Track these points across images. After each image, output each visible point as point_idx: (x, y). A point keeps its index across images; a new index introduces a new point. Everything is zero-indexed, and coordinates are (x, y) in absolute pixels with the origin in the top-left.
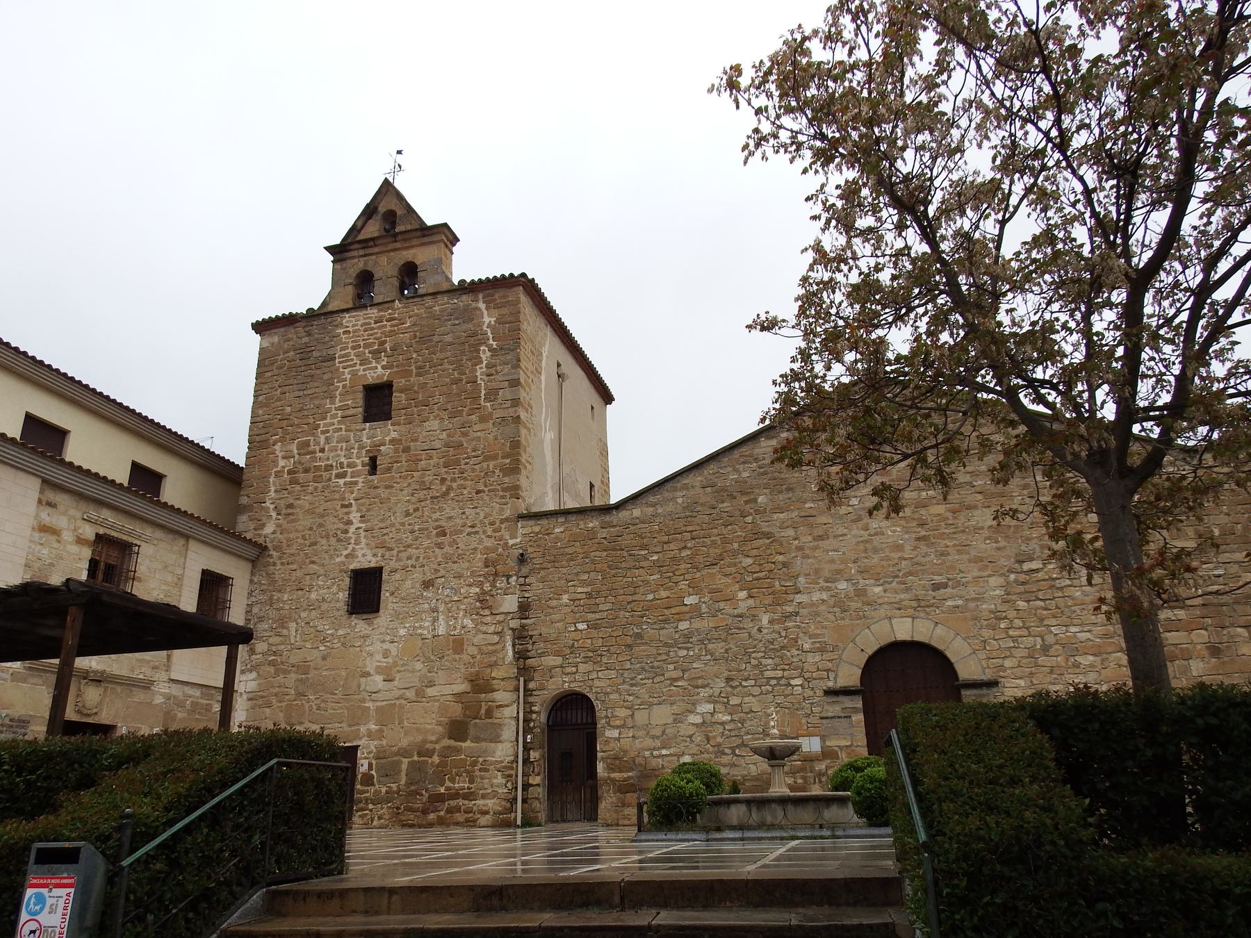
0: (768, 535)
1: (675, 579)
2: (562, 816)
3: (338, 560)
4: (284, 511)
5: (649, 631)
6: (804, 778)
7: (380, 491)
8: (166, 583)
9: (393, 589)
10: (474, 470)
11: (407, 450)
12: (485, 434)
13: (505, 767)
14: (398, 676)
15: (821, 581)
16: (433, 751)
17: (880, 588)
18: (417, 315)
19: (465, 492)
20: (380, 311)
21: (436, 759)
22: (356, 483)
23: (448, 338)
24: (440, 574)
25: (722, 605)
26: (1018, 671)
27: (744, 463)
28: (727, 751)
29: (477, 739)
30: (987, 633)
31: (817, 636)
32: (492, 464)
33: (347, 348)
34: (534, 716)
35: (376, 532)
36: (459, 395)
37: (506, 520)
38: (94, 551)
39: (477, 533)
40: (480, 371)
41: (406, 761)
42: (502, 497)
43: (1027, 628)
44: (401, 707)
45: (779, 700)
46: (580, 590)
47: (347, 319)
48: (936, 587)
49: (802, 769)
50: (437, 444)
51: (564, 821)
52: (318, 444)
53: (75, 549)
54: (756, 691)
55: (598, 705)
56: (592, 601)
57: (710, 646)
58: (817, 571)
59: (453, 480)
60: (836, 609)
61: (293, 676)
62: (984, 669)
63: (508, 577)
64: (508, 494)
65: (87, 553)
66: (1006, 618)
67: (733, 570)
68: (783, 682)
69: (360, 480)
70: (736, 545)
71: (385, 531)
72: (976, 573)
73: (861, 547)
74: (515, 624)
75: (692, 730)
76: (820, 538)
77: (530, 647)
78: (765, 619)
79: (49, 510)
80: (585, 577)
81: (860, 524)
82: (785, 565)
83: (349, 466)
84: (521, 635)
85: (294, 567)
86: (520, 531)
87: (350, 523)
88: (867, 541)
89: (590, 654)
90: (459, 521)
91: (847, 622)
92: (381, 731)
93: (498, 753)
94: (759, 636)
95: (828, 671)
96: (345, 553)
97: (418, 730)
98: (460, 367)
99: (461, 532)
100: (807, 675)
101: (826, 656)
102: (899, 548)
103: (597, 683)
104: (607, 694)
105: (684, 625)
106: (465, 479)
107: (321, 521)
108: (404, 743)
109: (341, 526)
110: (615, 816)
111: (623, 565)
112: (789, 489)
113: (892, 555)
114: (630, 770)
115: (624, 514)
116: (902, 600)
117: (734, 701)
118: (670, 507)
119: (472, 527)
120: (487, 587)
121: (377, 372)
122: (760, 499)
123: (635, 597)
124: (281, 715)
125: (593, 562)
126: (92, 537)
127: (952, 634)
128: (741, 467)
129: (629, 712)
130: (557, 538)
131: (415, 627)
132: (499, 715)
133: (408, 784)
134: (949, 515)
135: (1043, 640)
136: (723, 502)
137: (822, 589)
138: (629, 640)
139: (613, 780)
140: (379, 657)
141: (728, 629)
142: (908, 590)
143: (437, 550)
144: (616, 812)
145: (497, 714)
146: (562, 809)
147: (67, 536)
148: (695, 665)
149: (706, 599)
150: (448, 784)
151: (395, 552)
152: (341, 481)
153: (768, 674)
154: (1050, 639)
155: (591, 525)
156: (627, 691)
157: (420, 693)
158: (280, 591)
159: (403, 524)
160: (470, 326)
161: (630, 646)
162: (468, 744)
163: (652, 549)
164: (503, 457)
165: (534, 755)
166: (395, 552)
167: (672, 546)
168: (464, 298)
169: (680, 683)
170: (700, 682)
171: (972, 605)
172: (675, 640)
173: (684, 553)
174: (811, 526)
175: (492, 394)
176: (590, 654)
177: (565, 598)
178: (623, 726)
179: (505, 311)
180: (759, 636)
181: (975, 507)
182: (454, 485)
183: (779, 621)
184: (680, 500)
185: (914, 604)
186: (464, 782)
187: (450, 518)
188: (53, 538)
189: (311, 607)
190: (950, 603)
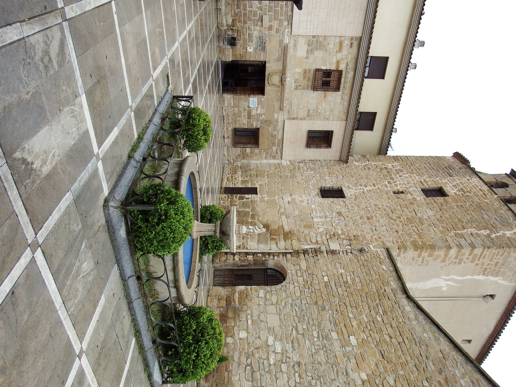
1: (367, 331)
2: (217, 275)
4: (366, 167)
5: (327, 315)
7: (385, 195)
8: (325, 113)
13: (244, 246)
19: (395, 226)
23: (486, 216)
25: (353, 361)
28: (249, 360)
32: (416, 237)
34: (272, 257)
36: (453, 222)
37: (384, 243)
38: (334, 70)
41: (250, 210)
42: (397, 242)
44: (276, 208)
46: (349, 278)
50: (419, 215)
51: (214, 277)
53: (334, 61)
55: (279, 286)
56: (342, 284)
57: (322, 352)
59: (401, 222)
61: (289, 174)
63: (350, 245)
64: (400, 244)
65: (333, 67)
67: (382, 370)
70: (402, 373)
74: (323, 248)
75: (263, 338)
77: (311, 255)
79: (349, 45)
80: (357, 280)
84: (316, 252)
86: (379, 250)
89: (309, 283)
90: (377, 224)
92: (264, 201)
93: (252, 243)
96: (350, 186)
103: (292, 286)
104: (286, 291)
105: (334, 335)
108: (258, 209)
110: (214, 294)
111: (370, 301)
114: (240, 303)
115: (404, 301)
117: (284, 367)
120: (342, 237)
123: (349, 307)
126: (340, 69)
130: (379, 267)
136: (434, 364)
138: (320, 303)
139: (234, 294)
140: (300, 199)
143: (359, 217)
144: (216, 296)
145: (272, 242)
146: (220, 275)
147: (339, 56)
148: (307, 342)
152: (386, 183)
155: (392, 283)
156: (288, 302)
157: (282, 214)
159: (370, 204)
161: (316, 303)
165: (250, 257)
166: (354, 202)
167: (390, 329)
169: (294, 332)
170: (296, 345)
172: (323, 330)
173: (388, 339)
175: (462, 236)
176: (309, 283)
187: (378, 221)
188: (337, 49)
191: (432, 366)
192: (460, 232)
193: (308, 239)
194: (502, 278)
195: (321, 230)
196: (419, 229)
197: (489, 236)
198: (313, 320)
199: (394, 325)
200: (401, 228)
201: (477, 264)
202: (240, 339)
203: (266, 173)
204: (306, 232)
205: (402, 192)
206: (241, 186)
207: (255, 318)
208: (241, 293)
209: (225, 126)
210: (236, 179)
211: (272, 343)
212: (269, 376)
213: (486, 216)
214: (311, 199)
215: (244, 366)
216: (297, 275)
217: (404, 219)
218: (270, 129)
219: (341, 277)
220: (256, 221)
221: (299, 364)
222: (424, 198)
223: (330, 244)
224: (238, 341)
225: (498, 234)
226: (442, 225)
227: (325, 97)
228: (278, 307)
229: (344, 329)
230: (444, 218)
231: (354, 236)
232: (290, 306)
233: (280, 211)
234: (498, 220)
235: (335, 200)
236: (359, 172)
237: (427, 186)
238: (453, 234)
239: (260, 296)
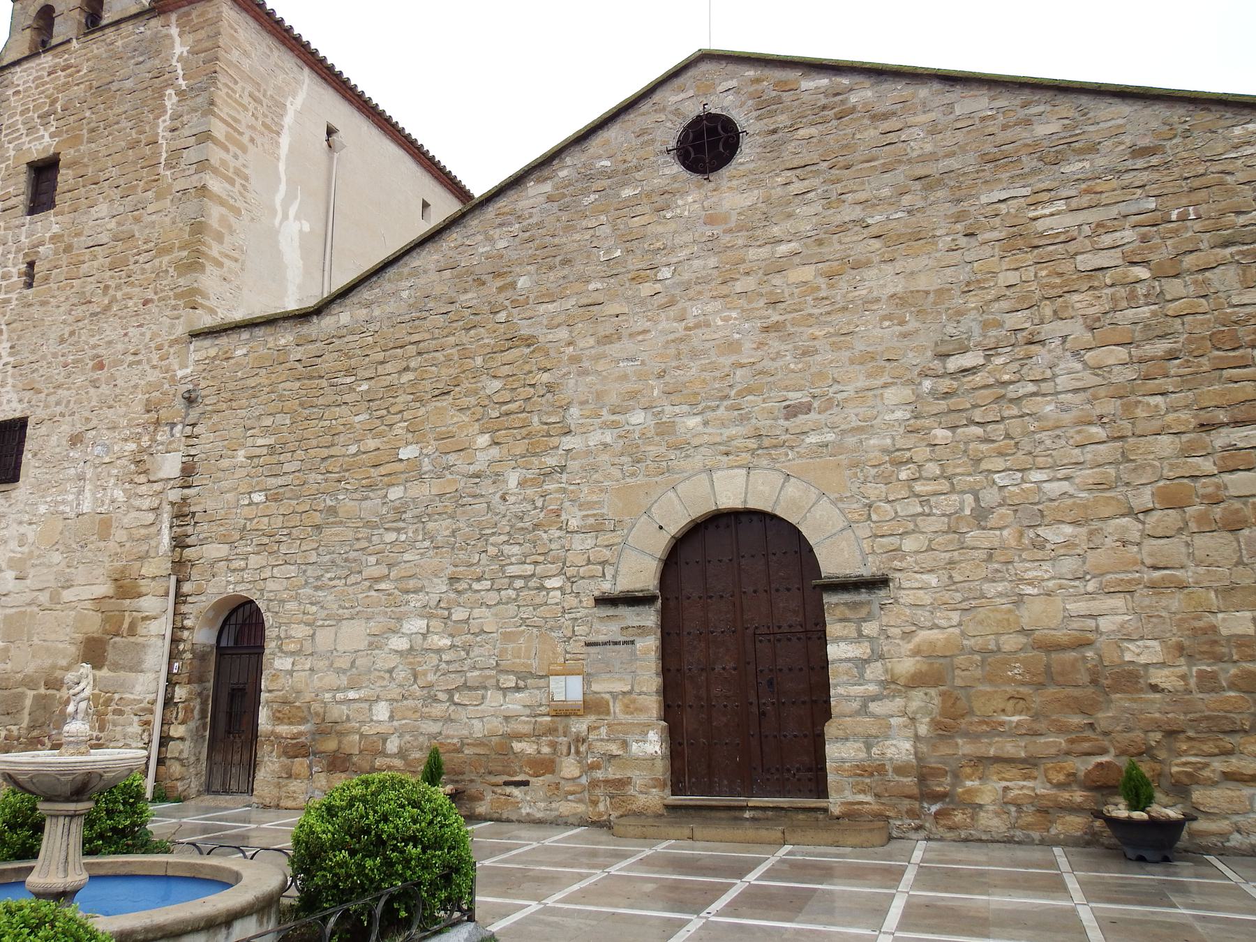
0: (529, 341)
1: (390, 419)
2: (224, 784)
5: (347, 504)
6: (553, 745)
7: (33, 310)
9: (36, 448)
10: (143, 271)
11: (68, 249)
13: (143, 710)
15: (604, 412)
17: (698, 419)
18: (96, 57)
19: (131, 303)
20: (55, 56)
23: (129, 84)
24: (90, 426)
25: (452, 458)
26: (927, 559)
27: (501, 225)
28: (442, 696)
29: (115, 667)
30: (874, 491)
31: (590, 505)
32: (166, 259)
33: (14, 114)
34: (186, 634)
35: (26, 369)
36: (135, 163)
37: (176, 341)
40: (164, 123)
41: (31, 693)
42: (175, 308)
43: (949, 478)
44: (33, 615)
45: (526, 612)
46: (260, 442)
48: (792, 411)
49: (552, 731)
50: (104, 238)
51: (227, 792)
54: (492, 597)
55: (268, 619)
56: (275, 459)
57: (430, 525)
58: (599, 396)
59: (118, 287)
60: (625, 459)
62: (864, 556)
64: (181, 303)
66: (910, 461)
67: (473, 400)
68: (531, 584)
69: (14, 296)
70: (479, 361)
71: (35, 366)
72: (862, 383)
73: (672, 351)
74: (175, 495)
75: (393, 661)
76: (607, 340)
77: (189, 530)
78: (513, 479)
80: (268, 421)
81: (672, 312)
82: (550, 388)
84: (182, 514)
86: (193, 357)
88: (681, 340)
89: (265, 540)
90: (120, 347)
91: (641, 479)
93: (138, 688)
94: (502, 508)
95: (603, 563)
97: (48, 649)
98: (138, 123)
100: (571, 571)
101: (604, 539)
102: (732, 347)
103: (271, 585)
104: (283, 601)
105: (395, 493)
108: (30, 669)
110: (275, 792)
111: (321, 401)
112: (566, 262)
113: (722, 360)
114: (304, 721)
115: (326, 323)
116: (731, 439)
117: (459, 614)
118: (391, 307)
122: (522, 282)
123: (333, 451)
125: (281, 398)
127: (813, 494)
128: (496, 233)
129: (308, 631)
130: (237, 364)
131: (56, 503)
132: (144, 632)
133: (32, 727)
134: (822, 282)
135: (977, 500)
136: (466, 291)
137: (606, 426)
138: (318, 518)
140: (13, 545)
141: (457, 496)
142: (744, 419)
143: (92, 390)
144: (279, 786)
145: (141, 629)
146: (225, 774)
148: (407, 557)
149: (429, 450)
153: (512, 570)
154: (990, 497)
155: (283, 342)
156: (310, 597)
157: (55, 598)
159: (55, 355)
160: (157, 62)
161: (318, 527)
163: (362, 373)
164: (181, 248)
165: (180, 693)
166: (43, 395)
167: (389, 368)
168: (153, 22)
169: (383, 586)
171: (851, 440)
172: (382, 517)
173: (409, 376)
174: (595, 320)
175: (175, 154)
176: (265, 540)
177: (241, 455)
178: (298, 653)
179: (202, 34)
180: (502, 508)
181: (867, 264)
182: (119, 295)
183: (534, 482)
184: (405, 295)
185: (752, 444)
187: (110, 342)
190: (813, 439)
191: (470, 295)
192: (164, 155)
193: (143, 531)
194: (290, 99)
195: (119, 495)
196: (145, 247)
197: (180, 93)
198: (358, 539)
199: (381, 356)
200: (137, 290)
201: (252, 140)
202: (392, 718)
204: (120, 535)
205: (31, 265)
207: (344, 680)
208: (277, 719)
211: (405, 640)
212: (476, 649)
213: (129, 84)
214: (19, 512)
215: (453, 707)
216: (243, 570)
217: (112, 277)
219: (255, 460)
221: (453, 579)
222: (55, 215)
223: (162, 475)
224: (395, 723)
225: (180, 72)
226: (139, 190)
228: (320, 623)
229: (383, 470)
230: (121, 181)
231: (148, 411)
232: (320, 593)
233: (47, 605)
234: (141, 59)
235: (28, 445)
237: (22, 198)
238: (168, 173)
239: (289, 667)
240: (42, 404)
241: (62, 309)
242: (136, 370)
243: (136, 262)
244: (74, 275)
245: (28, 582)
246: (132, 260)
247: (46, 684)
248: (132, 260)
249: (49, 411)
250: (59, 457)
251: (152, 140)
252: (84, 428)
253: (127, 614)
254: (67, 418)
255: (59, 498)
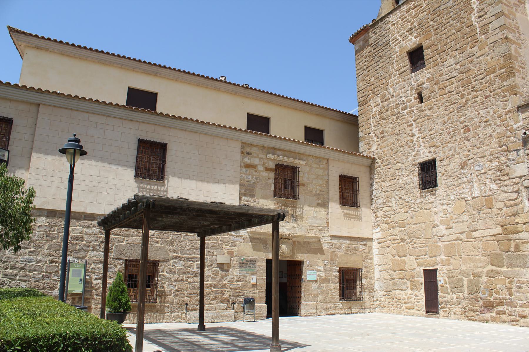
3: (410, 158)
4: (380, 136)
9: (443, 171)
10: (481, 84)
12: (490, 58)
14: (454, 226)
16: (482, 273)
19: (478, 99)
21: (485, 279)
22: (413, 111)
32: (492, 76)
38: (275, 174)
39: (490, 125)
47: (392, 18)
50: (455, 73)
52: (390, 93)
53: (265, 174)
59: (469, 94)
61: (398, 229)
63: (518, 150)
65: (272, 175)
71: (433, 136)
83: (407, 102)
85: (389, 166)
87: (413, 135)
96: (413, 153)
99: (480, 126)
106: (477, 91)
107: (398, 137)
109: (409, 138)
119: (486, 122)
120: (503, 160)
121: (412, 42)
124: (395, 251)
126: (274, 167)
140: (441, 214)
143: (466, 142)
147: (260, 168)
150: (495, 295)
151: (441, 148)
152: (405, 112)
158: (384, 182)
159: (443, 130)
162: (505, 269)
166: (441, 148)
182: (470, 97)
186: (505, 294)
187: (472, 119)
188: (253, 171)
189: (401, 189)
192: (478, 30)
193: (512, 202)
196: (479, 72)
200: (480, 92)
203: (397, 257)
206: (423, 291)
209: (338, 312)
210: (409, 298)
214: (440, 200)
217: (464, 90)
218: (340, 254)
220: (485, 270)
222: (427, 70)
223: (516, 175)
226: (468, 48)
227: (303, 185)
230: (458, 46)
231: (501, 147)
233: (466, 240)
235: (438, 170)
236: (389, 144)
237: (408, 66)
238: (483, 36)
240: (441, 152)
241: (440, 109)
242: (489, 129)
243: (475, 81)
244: (443, 93)
245: (453, 230)
246: (473, 80)
247: (473, 274)
248: (473, 80)
249: (446, 154)
250: (456, 173)
251: (470, 24)
252: (466, 159)
253: (512, 241)
254: (456, 156)
255: (460, 192)
